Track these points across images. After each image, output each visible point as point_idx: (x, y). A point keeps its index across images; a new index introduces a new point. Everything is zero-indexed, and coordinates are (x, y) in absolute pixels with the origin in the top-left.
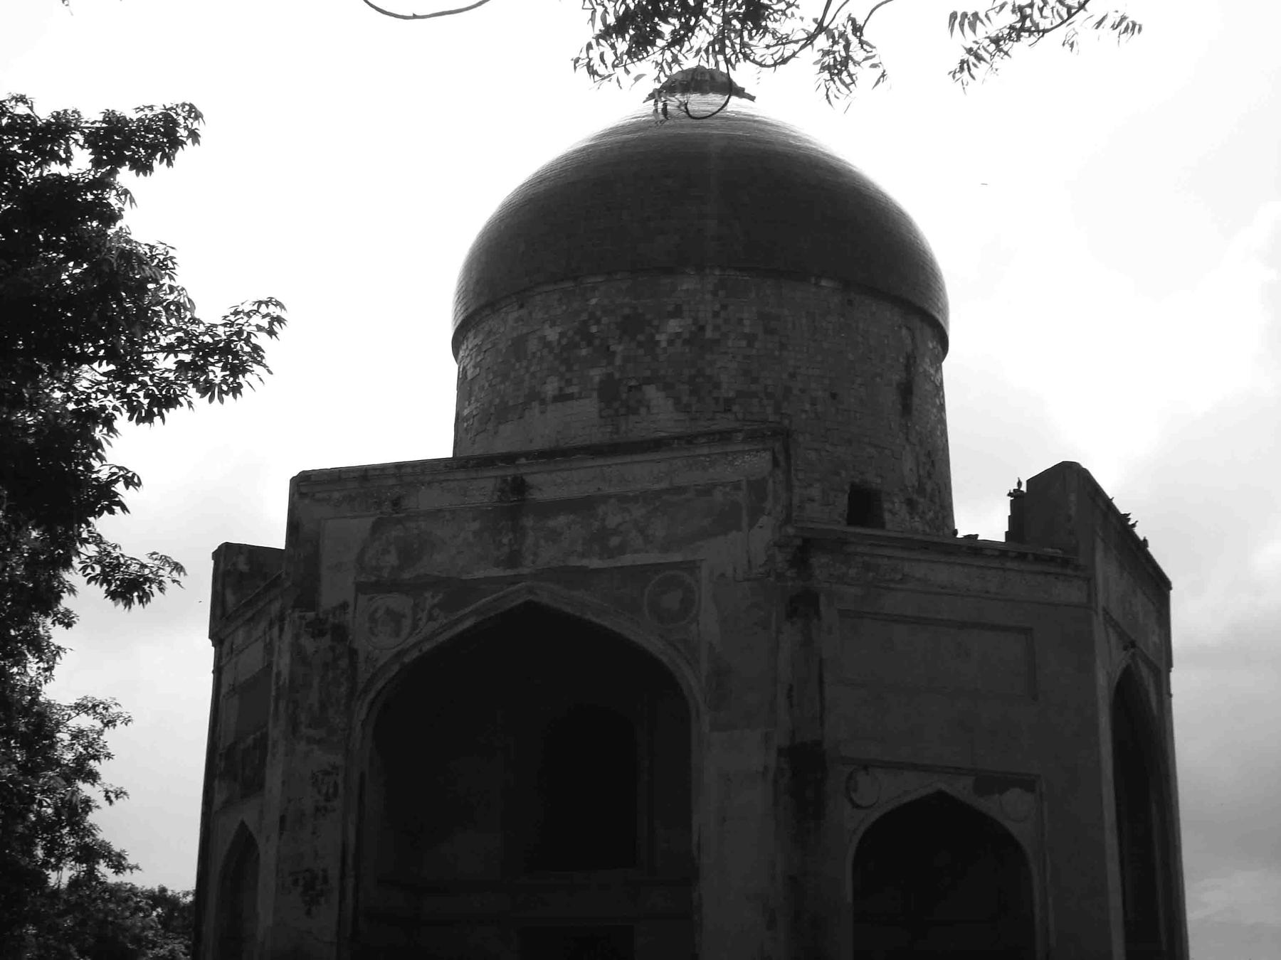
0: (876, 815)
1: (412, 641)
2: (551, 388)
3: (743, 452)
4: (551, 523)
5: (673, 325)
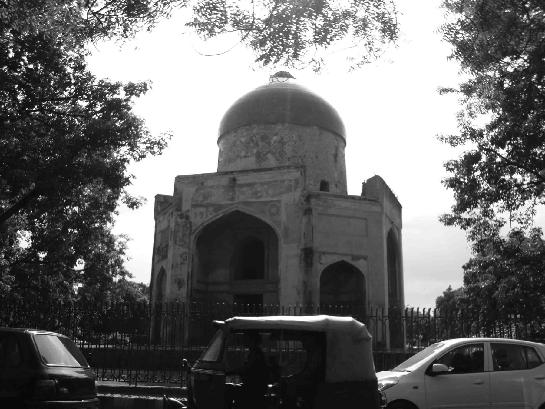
0: (326, 266)
1: (206, 220)
2: (243, 154)
3: (293, 171)
5: (275, 138)
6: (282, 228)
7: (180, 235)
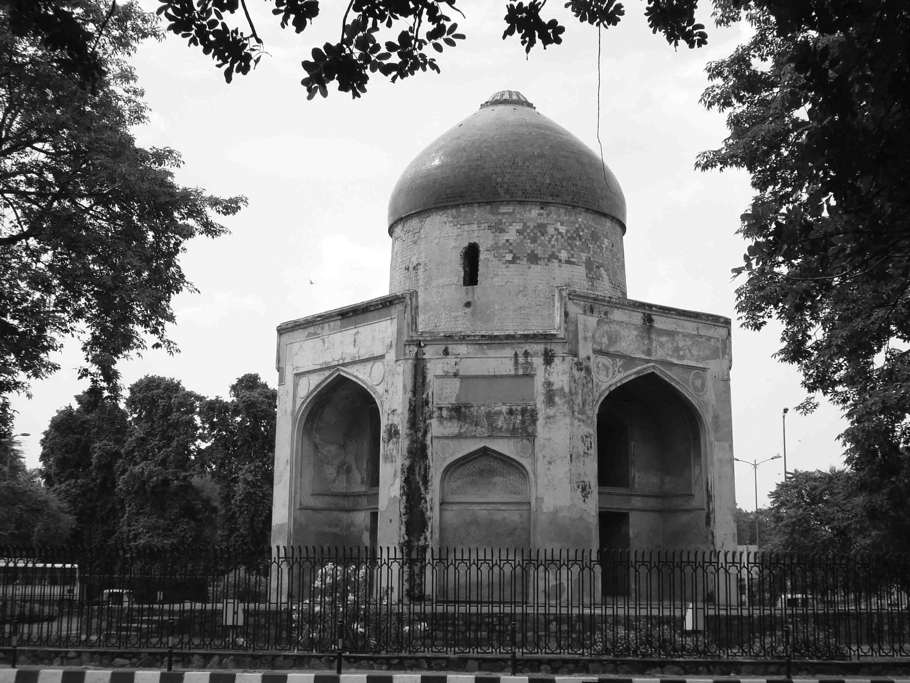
4: (661, 339)
6: (711, 414)
7: (579, 400)
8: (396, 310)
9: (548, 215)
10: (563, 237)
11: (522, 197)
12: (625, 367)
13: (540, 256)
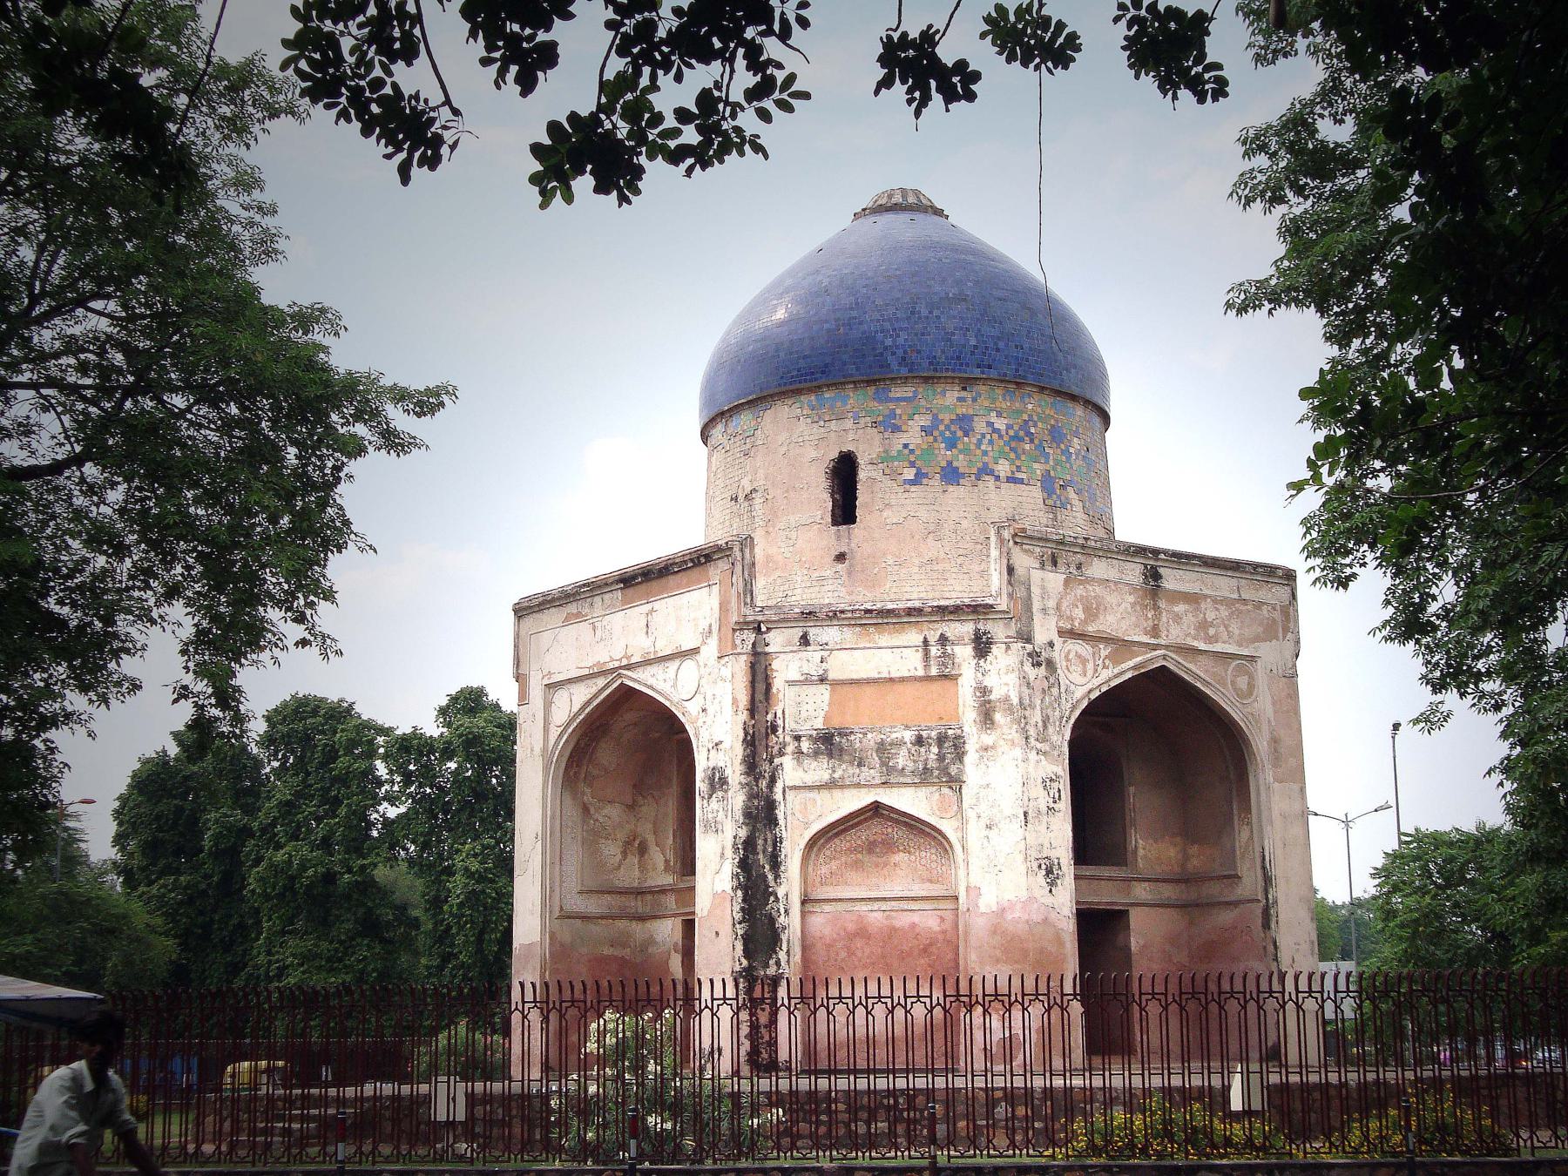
1: (1097, 682)
4: (1176, 609)
7: (1037, 717)
8: (717, 570)
9: (974, 400)
10: (1001, 437)
11: (929, 370)
12: (1115, 658)
13: (961, 470)
